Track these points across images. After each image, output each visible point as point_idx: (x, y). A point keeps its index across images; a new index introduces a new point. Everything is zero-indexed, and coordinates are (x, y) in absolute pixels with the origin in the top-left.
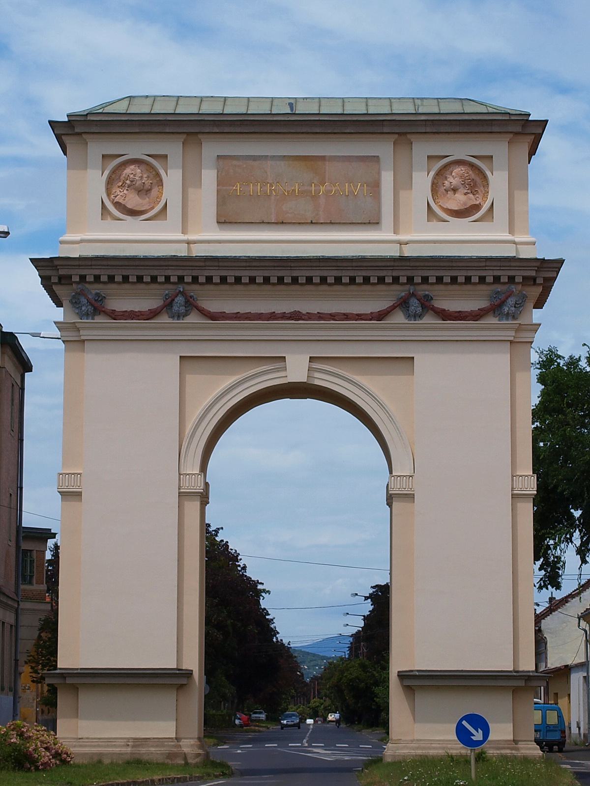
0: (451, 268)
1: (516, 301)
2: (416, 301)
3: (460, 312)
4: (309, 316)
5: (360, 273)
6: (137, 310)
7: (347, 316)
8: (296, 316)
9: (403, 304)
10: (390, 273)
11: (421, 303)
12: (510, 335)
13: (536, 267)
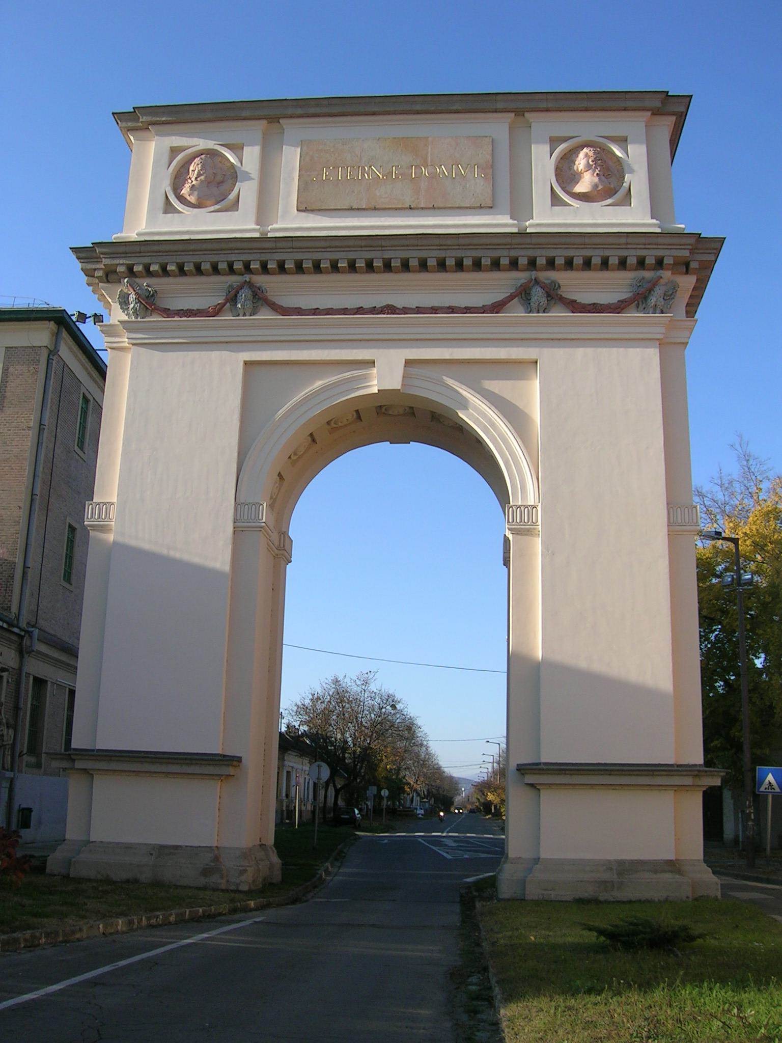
0: (584, 246)
1: (666, 292)
2: (539, 289)
3: (594, 304)
4: (405, 310)
5: (469, 253)
6: (195, 309)
7: (453, 309)
8: (390, 309)
9: (523, 294)
10: (505, 253)
11: (547, 292)
12: (658, 332)
13: (689, 245)
